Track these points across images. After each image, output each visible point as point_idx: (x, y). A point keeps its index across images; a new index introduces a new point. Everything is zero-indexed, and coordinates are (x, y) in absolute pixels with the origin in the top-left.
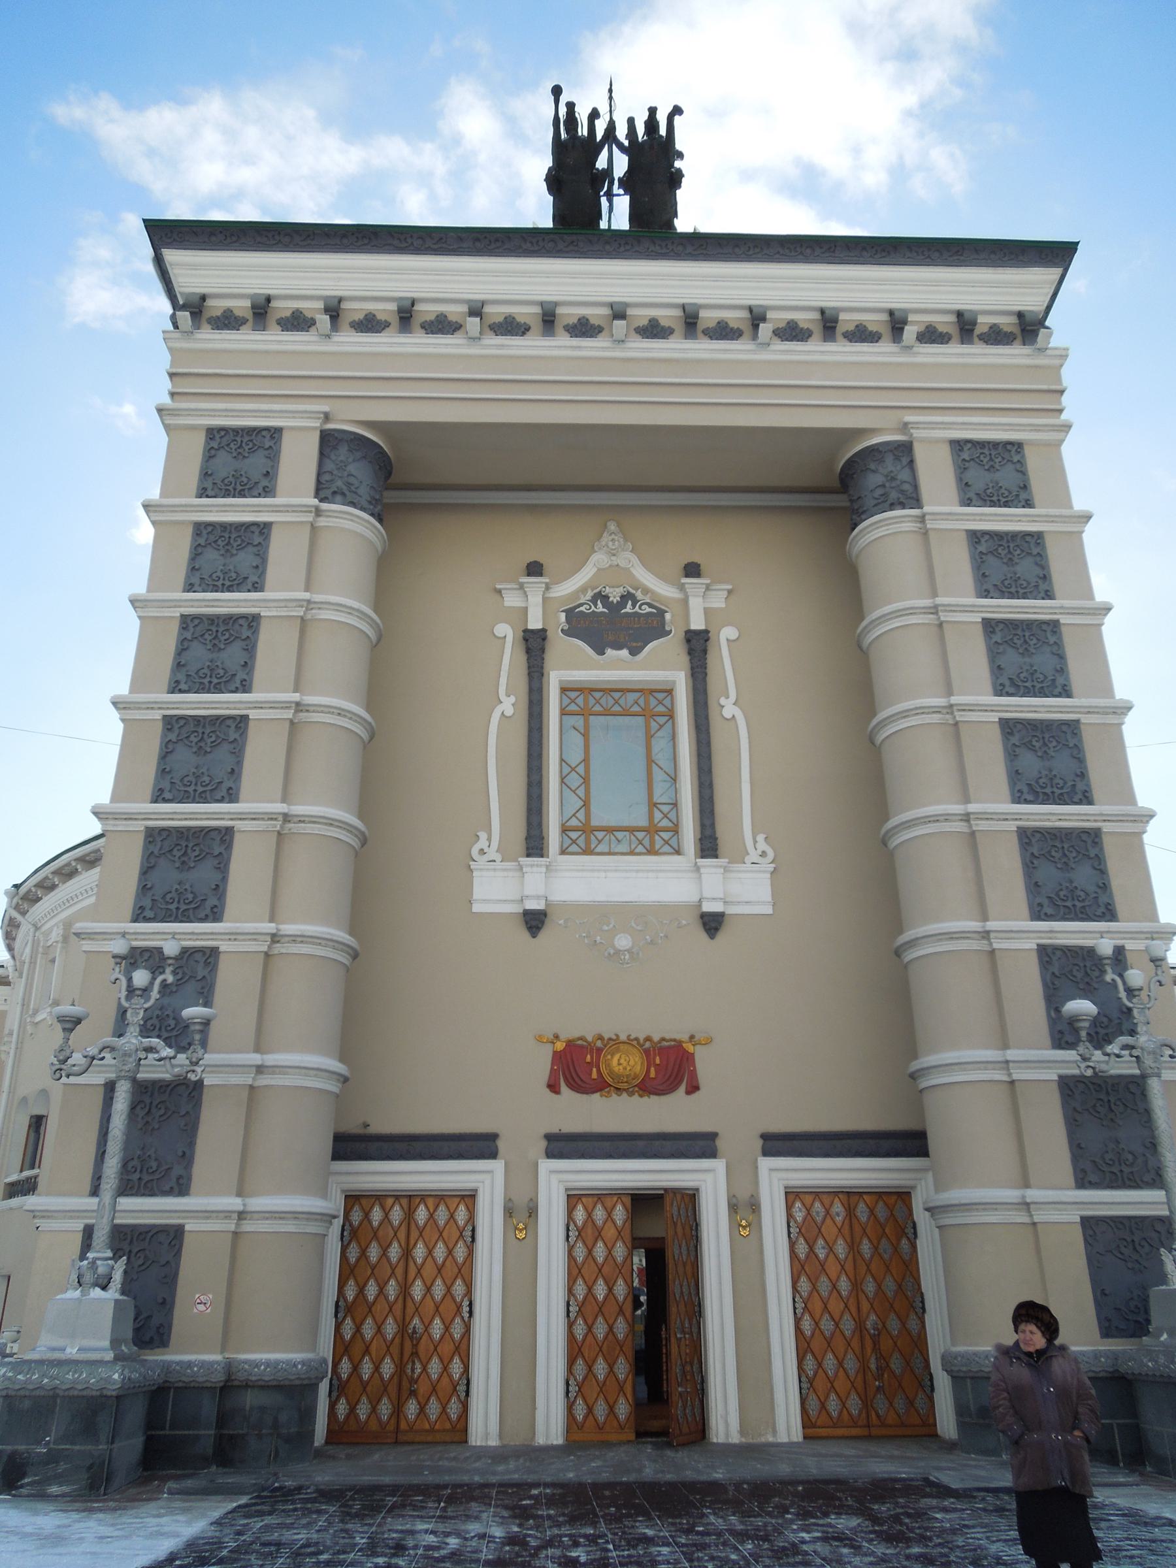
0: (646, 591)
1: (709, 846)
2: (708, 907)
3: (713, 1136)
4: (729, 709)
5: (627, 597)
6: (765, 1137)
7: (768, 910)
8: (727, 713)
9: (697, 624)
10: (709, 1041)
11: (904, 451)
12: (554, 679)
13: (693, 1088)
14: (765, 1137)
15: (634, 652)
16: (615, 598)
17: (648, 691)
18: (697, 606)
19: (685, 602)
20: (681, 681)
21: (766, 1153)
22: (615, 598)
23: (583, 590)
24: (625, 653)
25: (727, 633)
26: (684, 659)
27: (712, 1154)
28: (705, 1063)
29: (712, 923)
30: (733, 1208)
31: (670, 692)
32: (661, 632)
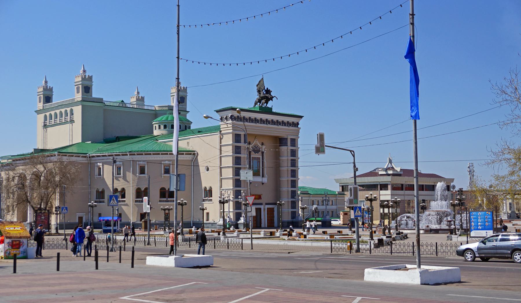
0: (259, 146)
1: (263, 176)
2: (263, 182)
3: (262, 203)
4: (265, 161)
5: (257, 147)
6: (266, 203)
7: (267, 182)
8: (265, 161)
9: (263, 151)
10: (262, 195)
11: (287, 139)
12: (251, 156)
13: (261, 199)
14: (266, 203)
15: (258, 153)
16: (256, 147)
17: (257, 158)
18: (263, 148)
19: (262, 148)
20: (261, 157)
21: (266, 205)
22: (256, 147)
23: (254, 145)
24: (257, 154)
25: (265, 152)
26: (261, 155)
27: (262, 205)
28: (262, 197)
29: (263, 184)
30: (264, 209)
31: (259, 158)
32: (259, 151)
